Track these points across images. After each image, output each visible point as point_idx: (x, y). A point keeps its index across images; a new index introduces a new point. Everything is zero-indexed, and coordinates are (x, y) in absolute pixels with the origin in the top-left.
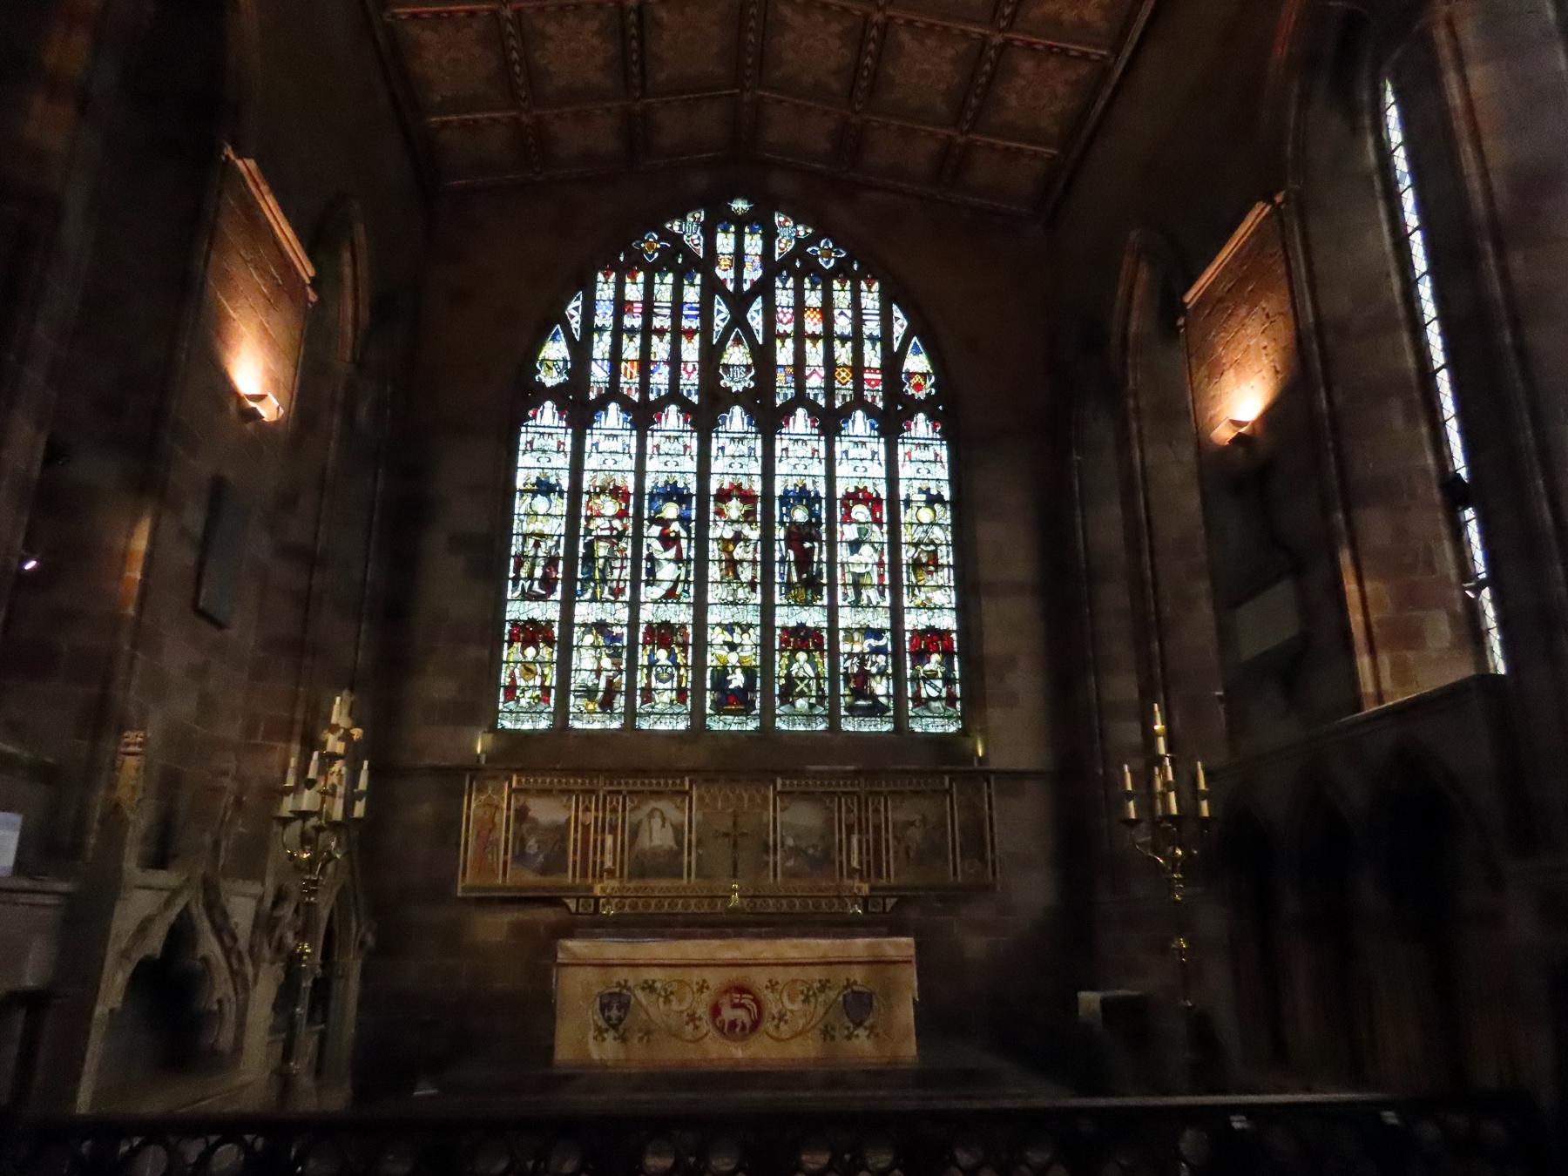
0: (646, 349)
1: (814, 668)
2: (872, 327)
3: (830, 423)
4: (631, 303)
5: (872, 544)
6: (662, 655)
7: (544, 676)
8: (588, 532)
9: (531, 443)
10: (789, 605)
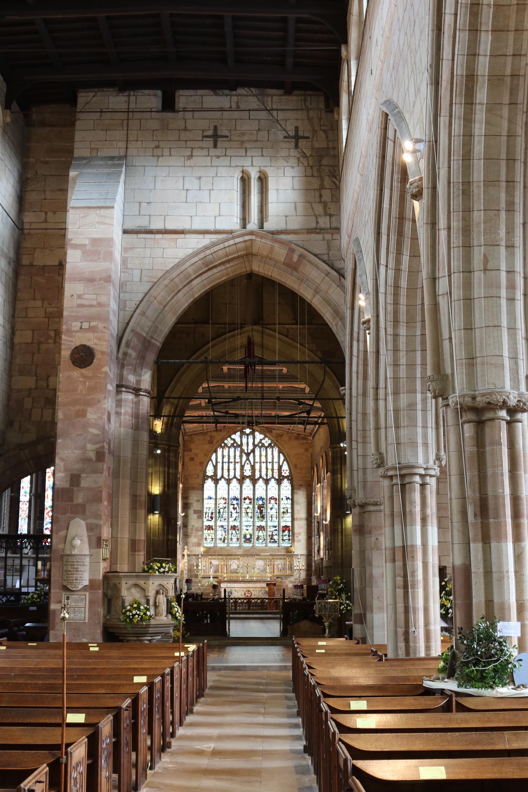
2: (276, 459)
6: (234, 532)
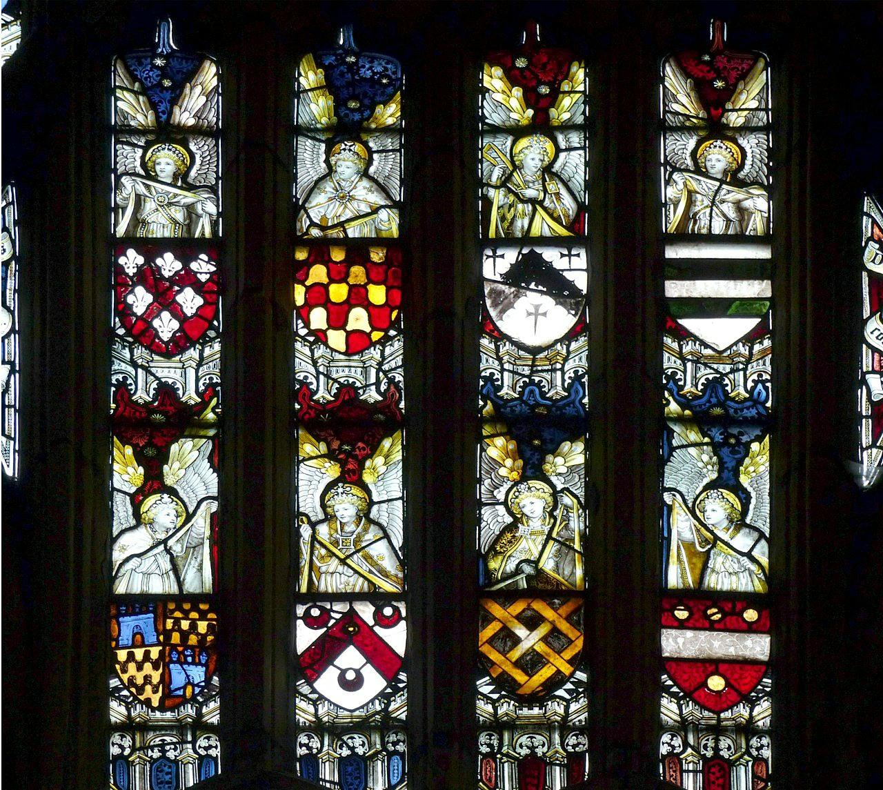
2: (721, 339)
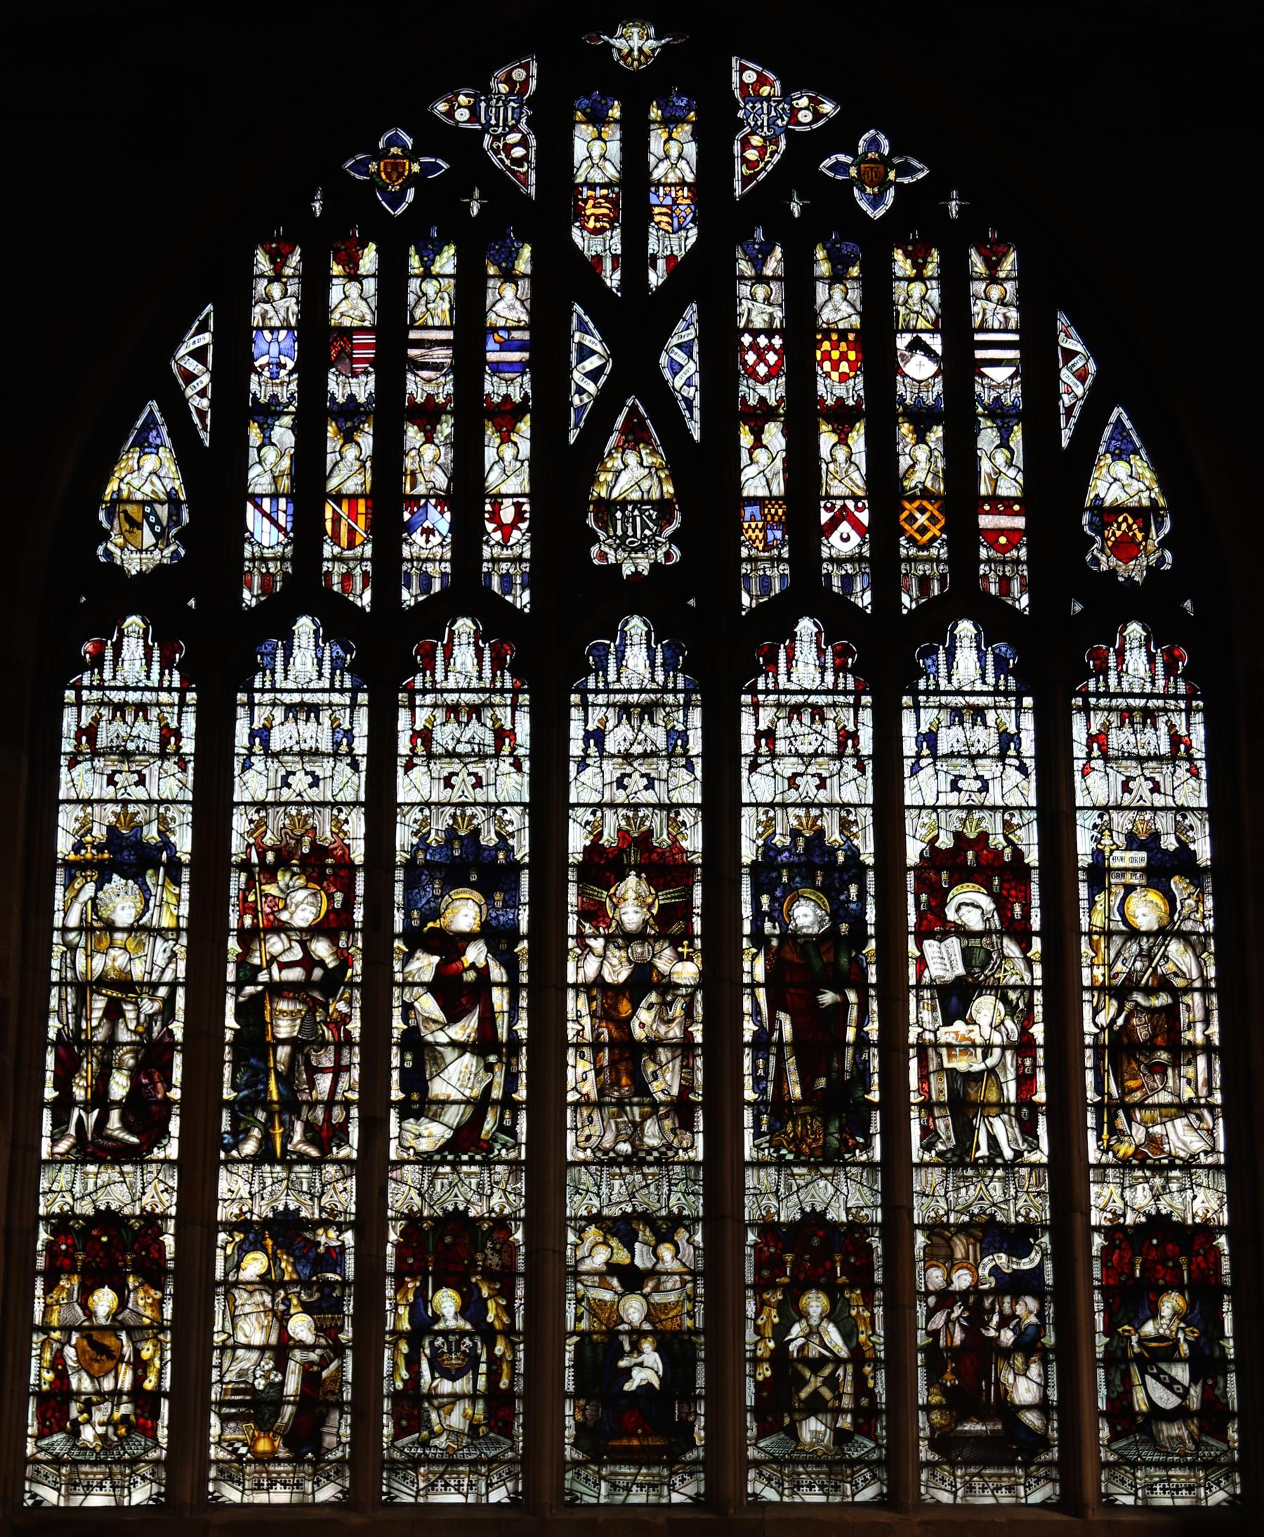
0: (388, 461)
1: (848, 1335)
2: (999, 379)
3: (886, 660)
4: (349, 332)
5: (1001, 992)
6: (447, 1302)
7: (140, 1366)
8: (248, 973)
9: (90, 732)
10: (780, 1164)
